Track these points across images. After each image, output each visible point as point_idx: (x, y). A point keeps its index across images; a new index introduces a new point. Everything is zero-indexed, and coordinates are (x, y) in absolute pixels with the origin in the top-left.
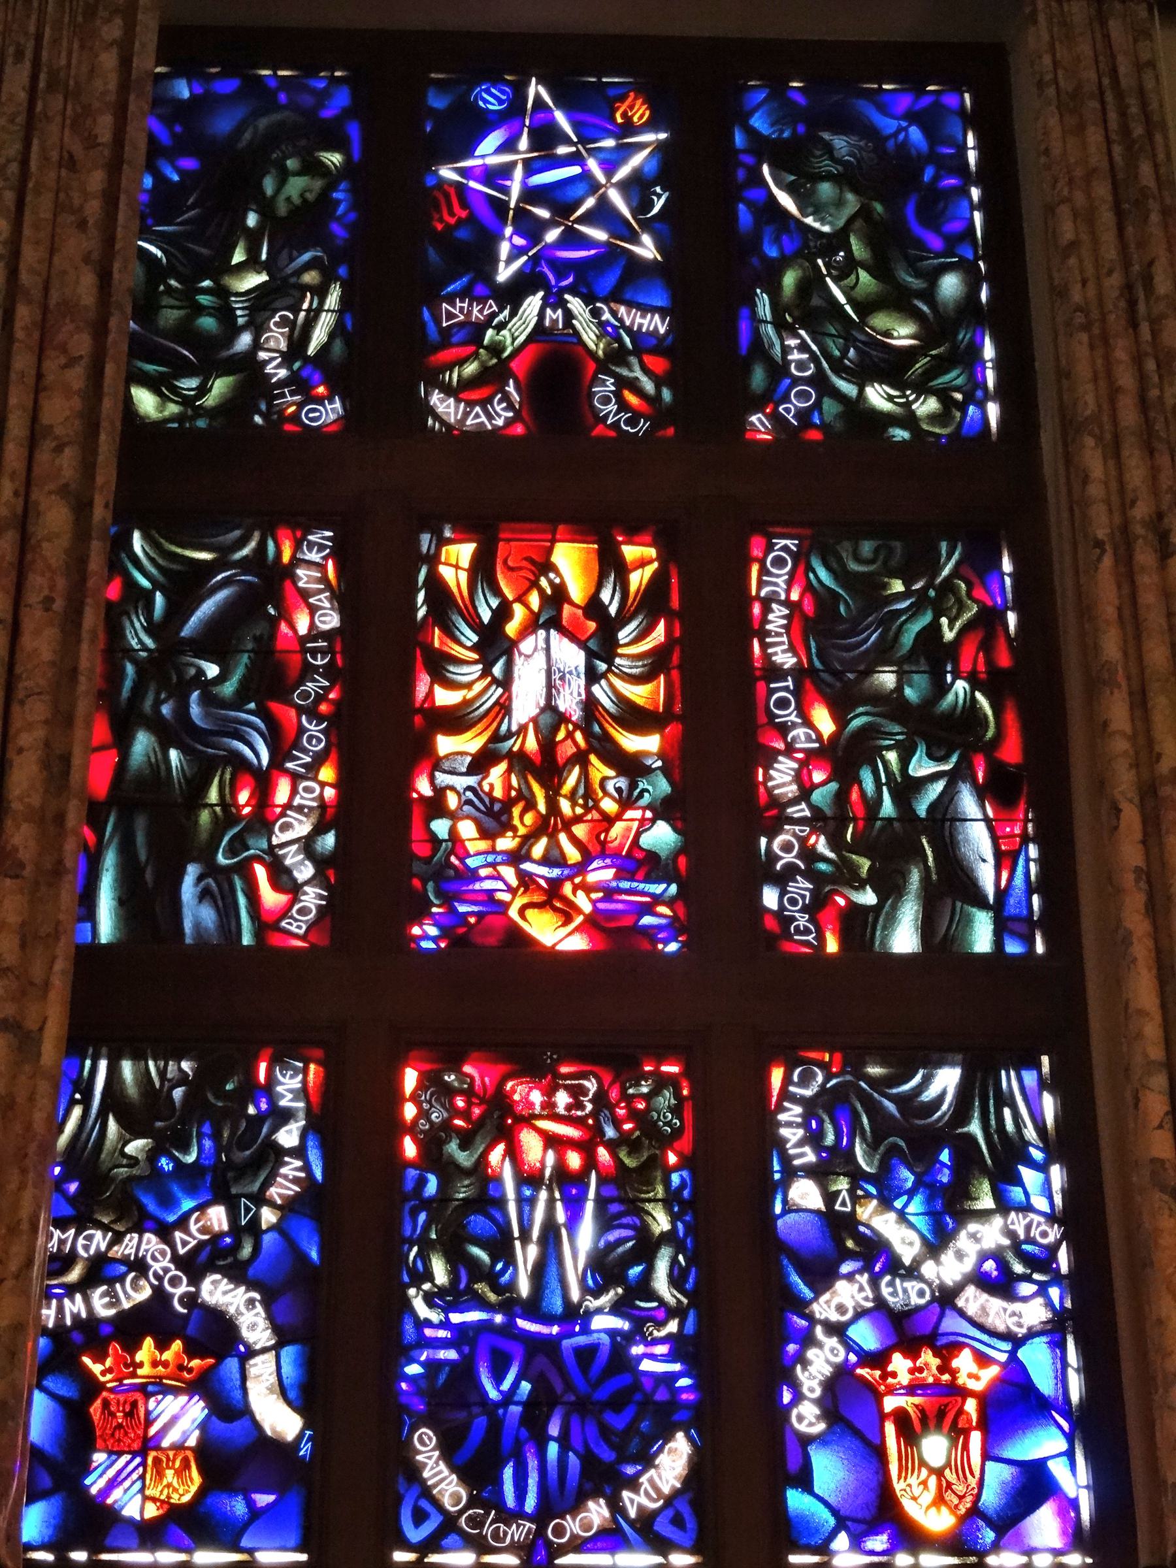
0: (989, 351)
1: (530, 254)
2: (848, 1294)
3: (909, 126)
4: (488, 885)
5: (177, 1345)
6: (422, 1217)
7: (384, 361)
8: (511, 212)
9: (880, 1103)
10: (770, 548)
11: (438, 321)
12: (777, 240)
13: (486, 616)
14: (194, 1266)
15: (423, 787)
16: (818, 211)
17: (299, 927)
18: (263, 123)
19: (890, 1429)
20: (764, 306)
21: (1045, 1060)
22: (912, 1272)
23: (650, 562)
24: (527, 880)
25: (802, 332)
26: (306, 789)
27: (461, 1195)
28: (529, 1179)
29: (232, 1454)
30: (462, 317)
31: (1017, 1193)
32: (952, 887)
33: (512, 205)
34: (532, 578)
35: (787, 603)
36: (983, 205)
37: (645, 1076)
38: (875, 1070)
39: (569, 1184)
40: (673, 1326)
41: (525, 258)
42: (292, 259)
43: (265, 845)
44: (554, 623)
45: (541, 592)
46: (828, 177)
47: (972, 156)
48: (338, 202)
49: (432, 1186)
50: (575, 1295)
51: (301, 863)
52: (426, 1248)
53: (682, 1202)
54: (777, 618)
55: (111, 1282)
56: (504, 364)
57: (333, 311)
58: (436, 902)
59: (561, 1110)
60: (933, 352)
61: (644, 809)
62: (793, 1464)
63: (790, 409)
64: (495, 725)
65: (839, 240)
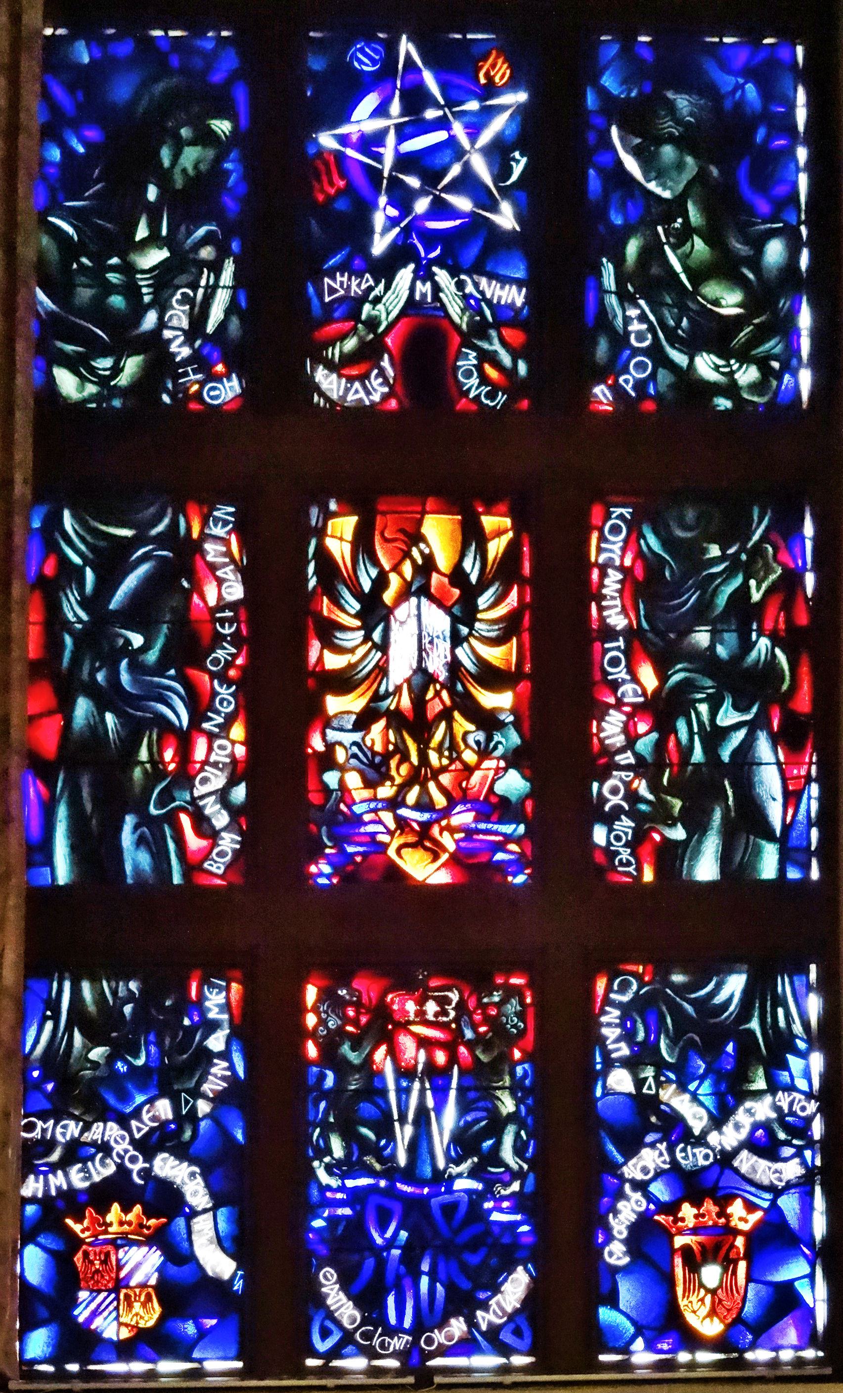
0: (805, 319)
1: (402, 225)
2: (651, 1158)
3: (746, 83)
4: (371, 828)
5: (138, 1209)
6: (323, 1105)
7: (276, 335)
8: (385, 181)
9: (681, 1005)
10: (608, 516)
11: (321, 296)
13: (366, 585)
14: (147, 1147)
15: (317, 743)
16: (660, 175)
17: (218, 868)
18: (159, 88)
19: (678, 1261)
20: (609, 278)
21: (813, 968)
22: (701, 1141)
23: (505, 531)
24: (402, 824)
25: (642, 302)
26: (222, 747)
27: (353, 1087)
28: (406, 1073)
29: (183, 1289)
30: (342, 292)
31: (784, 1076)
32: (748, 821)
33: (386, 174)
34: (405, 548)
35: (622, 569)
36: (810, 166)
38: (678, 978)
39: (436, 1077)
40: (516, 1186)
41: (397, 230)
42: (190, 233)
43: (188, 798)
44: (424, 591)
45: (414, 562)
46: (671, 139)
47: (801, 116)
48: (228, 173)
49: (330, 1080)
50: (441, 1163)
51: (219, 812)
52: (327, 1129)
53: (523, 1088)
54: (612, 582)
55: (84, 1161)
56: (380, 339)
57: (228, 287)
58: (329, 844)
59: (430, 1017)
60: (756, 321)
61: (498, 759)
62: (605, 1288)
63: (627, 381)
64: (375, 685)
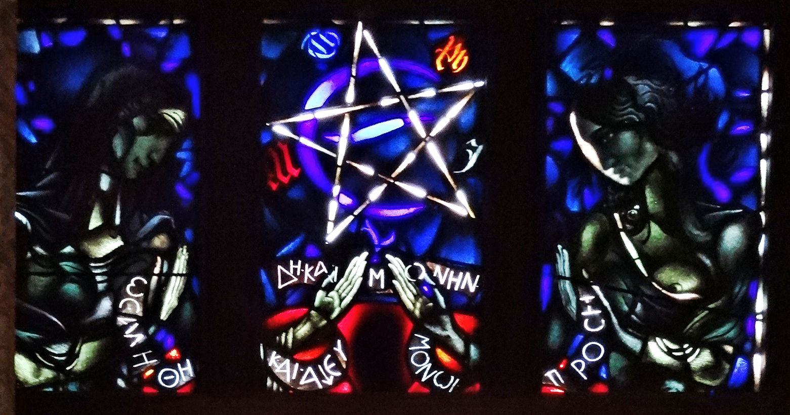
0: (761, 303)
1: (356, 213)
3: (709, 68)
8: (339, 170)
11: (275, 284)
12: (579, 195)
18: (111, 77)
20: (564, 264)
25: (596, 288)
30: (296, 279)
33: (340, 162)
41: (350, 218)
42: (143, 224)
46: (630, 126)
47: (766, 100)
48: (181, 162)
56: (333, 323)
57: (181, 275)
60: (711, 306)
63: (580, 366)
65: (635, 192)
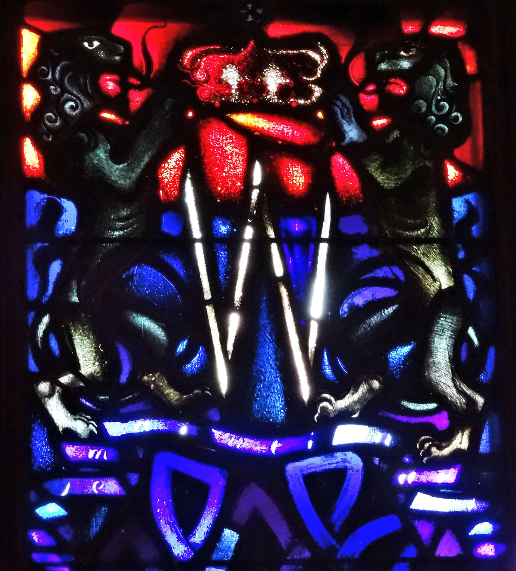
6: (55, 268)
27: (117, 233)
37: (407, 42)
40: (461, 441)
53: (470, 244)
